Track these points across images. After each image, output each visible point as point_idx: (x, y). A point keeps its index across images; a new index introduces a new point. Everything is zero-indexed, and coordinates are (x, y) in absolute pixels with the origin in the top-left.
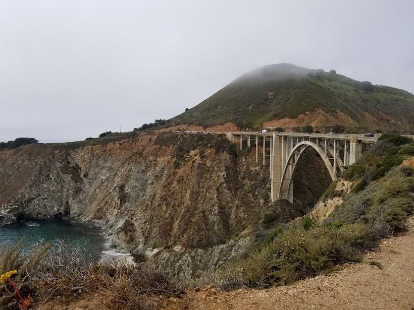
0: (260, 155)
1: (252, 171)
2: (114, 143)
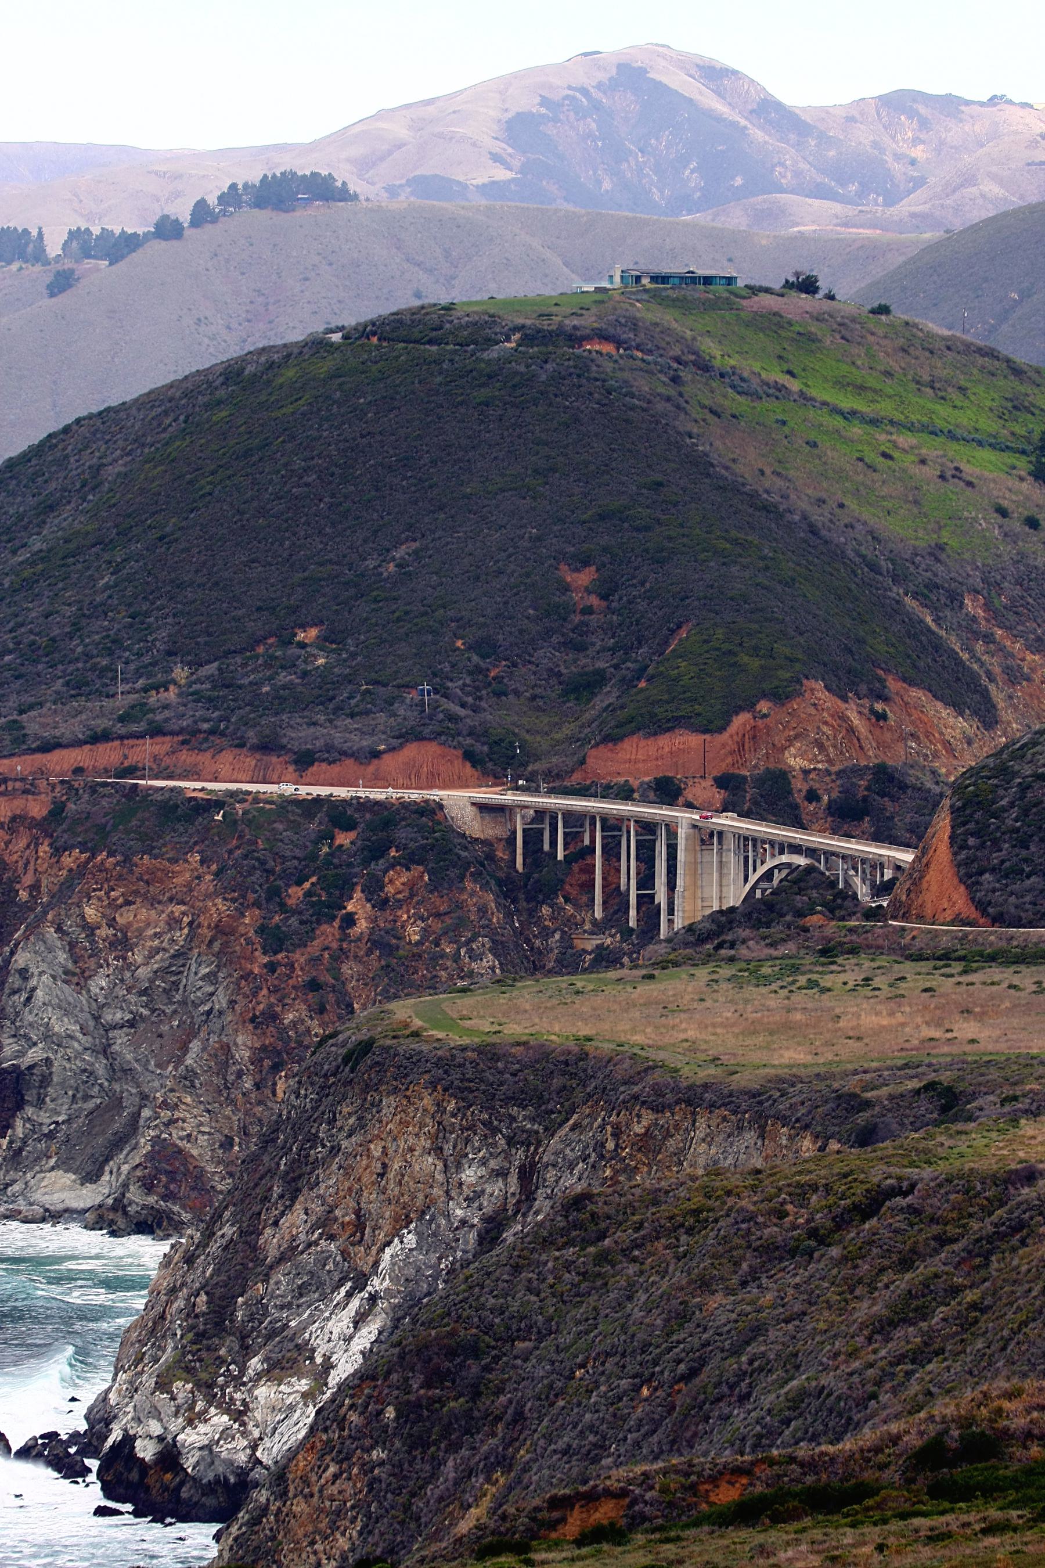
0: (615, 897)
1: (584, 951)
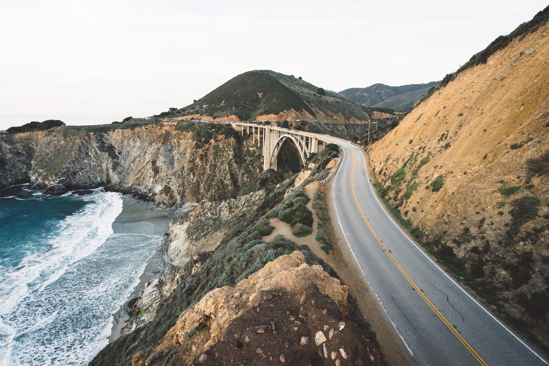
0: (256, 140)
2: (141, 128)
